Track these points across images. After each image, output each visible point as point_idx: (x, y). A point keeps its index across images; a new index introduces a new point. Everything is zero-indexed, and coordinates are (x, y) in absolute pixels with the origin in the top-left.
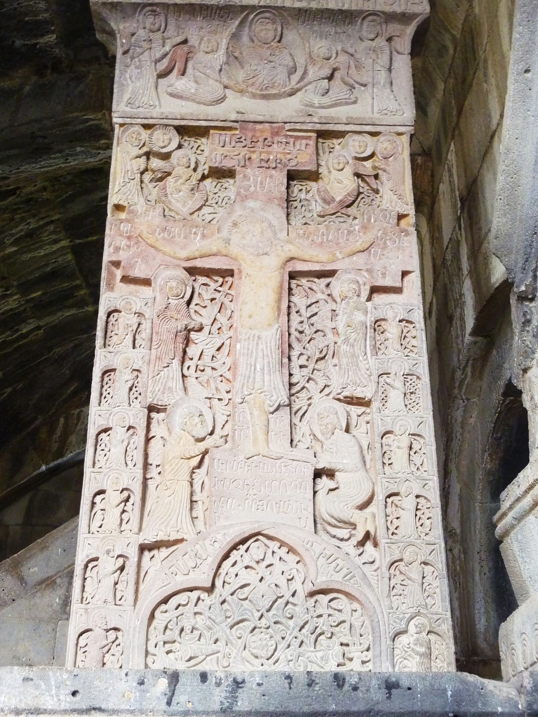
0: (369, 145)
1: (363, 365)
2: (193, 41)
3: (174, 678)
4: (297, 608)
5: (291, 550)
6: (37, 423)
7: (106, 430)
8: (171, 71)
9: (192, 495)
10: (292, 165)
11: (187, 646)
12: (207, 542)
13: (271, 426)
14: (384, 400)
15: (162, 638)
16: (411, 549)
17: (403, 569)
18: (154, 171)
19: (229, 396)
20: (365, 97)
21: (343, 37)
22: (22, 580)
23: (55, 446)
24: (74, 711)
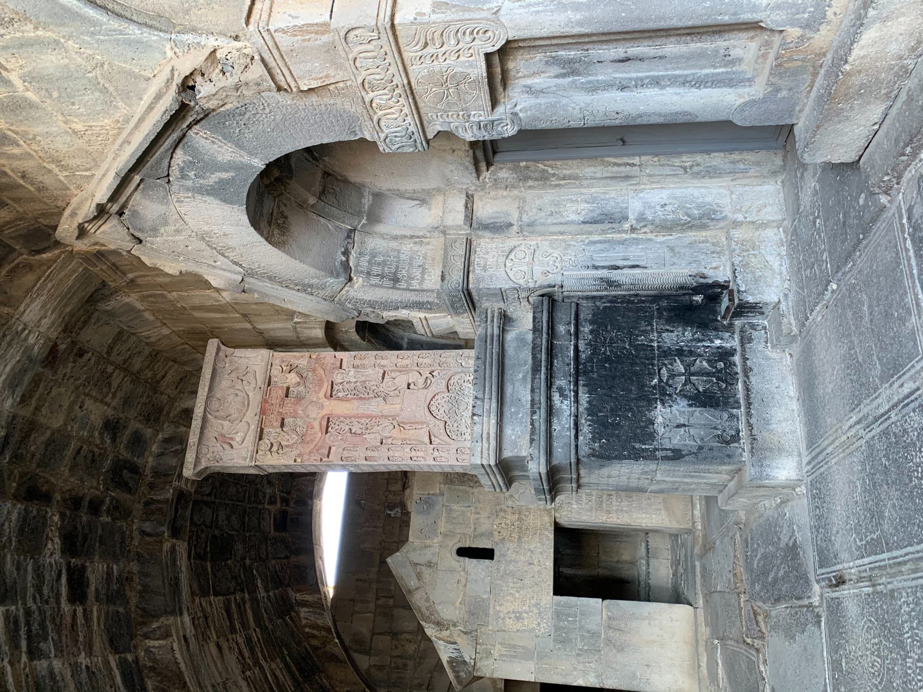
2: (216, 435)
3: (474, 415)
11: (463, 429)
14: (384, 366)
23: (323, 633)
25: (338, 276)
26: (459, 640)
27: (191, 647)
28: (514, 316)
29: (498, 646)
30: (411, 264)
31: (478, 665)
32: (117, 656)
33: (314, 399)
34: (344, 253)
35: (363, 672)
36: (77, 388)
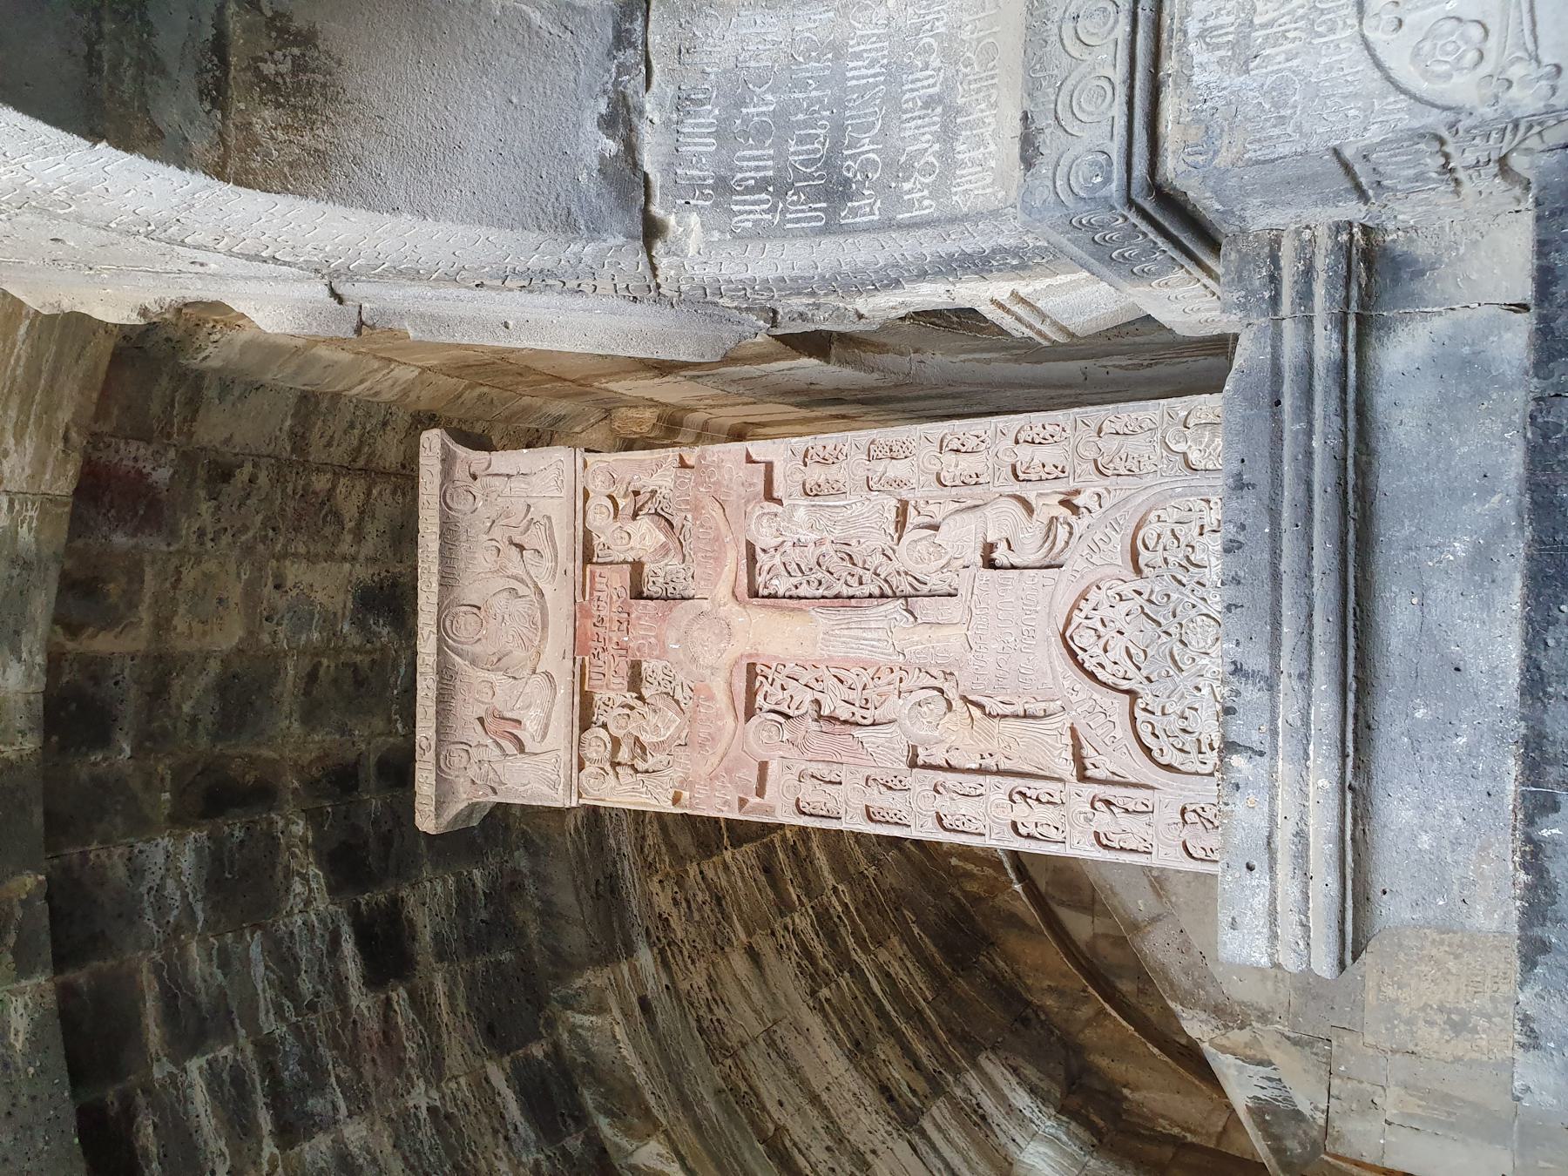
0: (599, 502)
1: (857, 509)
3: (1229, 747)
4: (1157, 589)
5: (1083, 597)
6: (958, 894)
7: (940, 820)
8: (516, 737)
9: (1017, 716)
10: (625, 594)
12: (1074, 698)
13: (932, 620)
14: (900, 484)
15: (1194, 754)
16: (1081, 450)
17: (1106, 459)
18: (634, 758)
19: (896, 669)
20: (542, 508)
21: (472, 532)
22: (1154, 920)
23: (989, 871)
24: (1272, 869)
25: (595, 230)
26: (1277, 1057)
27: (659, 1018)
28: (1422, 249)
29: (1394, 1092)
30: (893, 102)
31: (1337, 1123)
32: (507, 1060)
33: (706, 605)
34: (608, 124)
35: (1084, 948)
36: (248, 550)
